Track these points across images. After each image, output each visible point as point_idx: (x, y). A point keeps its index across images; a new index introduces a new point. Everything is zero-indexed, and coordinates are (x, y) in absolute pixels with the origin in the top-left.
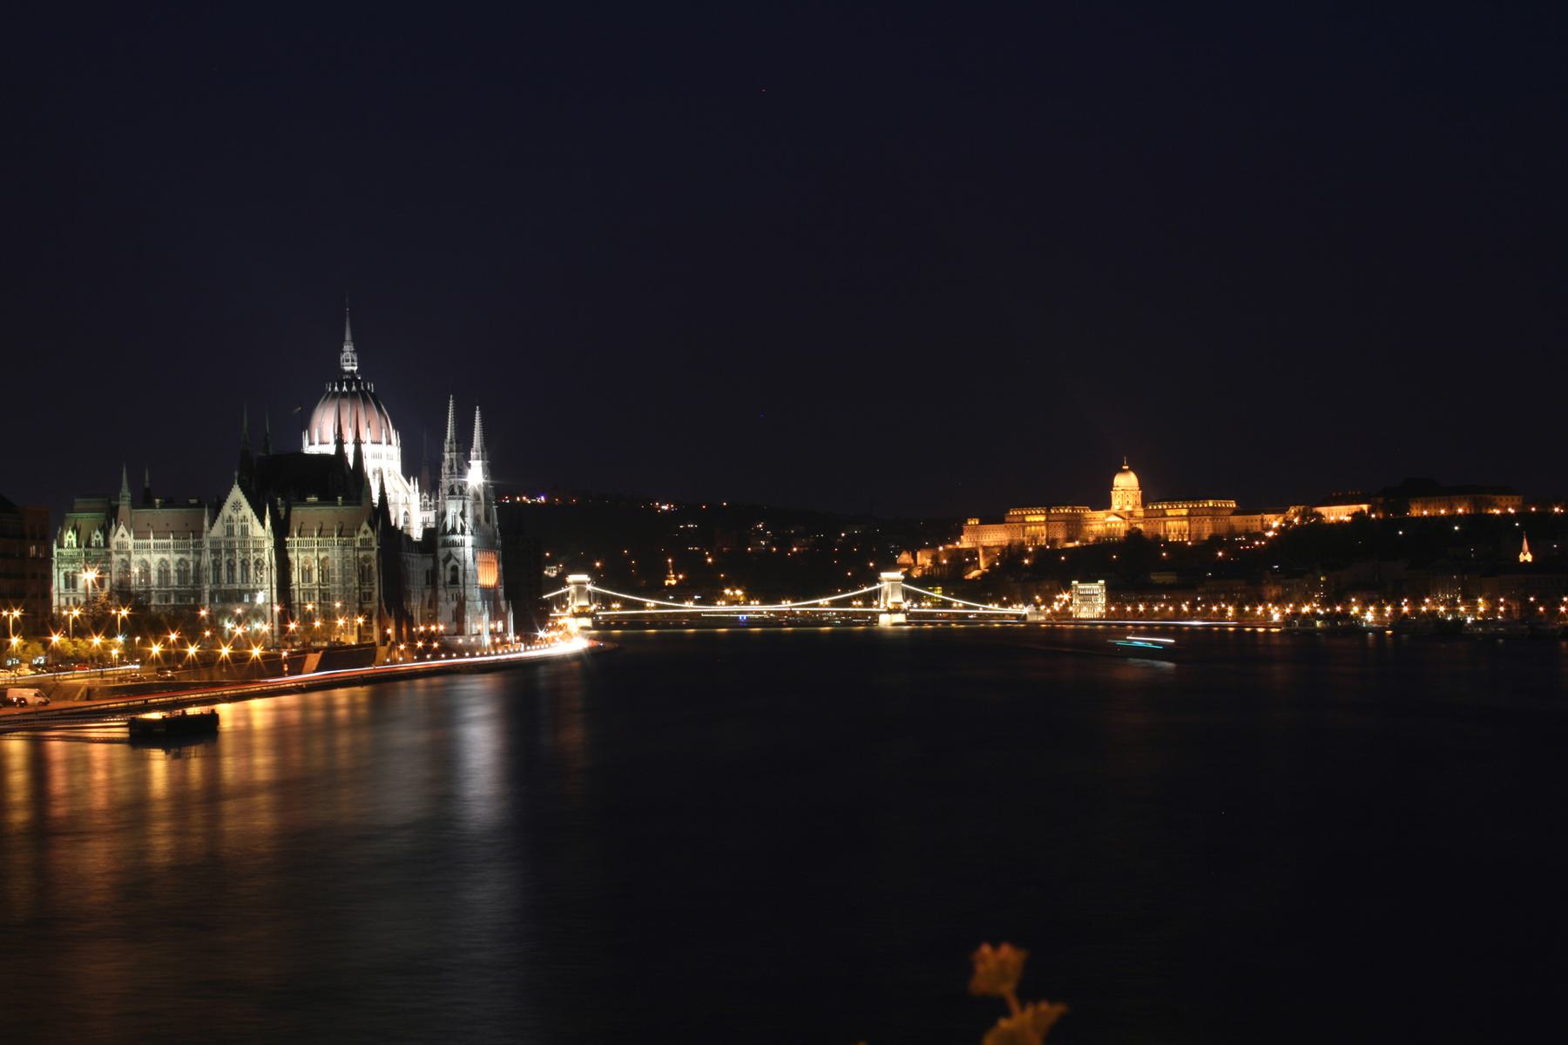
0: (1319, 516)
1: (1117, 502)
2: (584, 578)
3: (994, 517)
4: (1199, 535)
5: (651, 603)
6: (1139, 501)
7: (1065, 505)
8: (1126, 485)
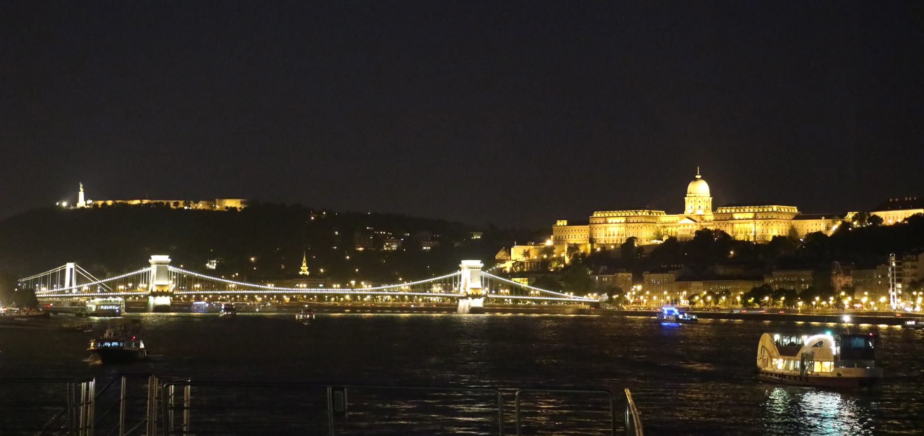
0: (880, 220)
1: (690, 205)
2: (165, 258)
3: (581, 219)
4: (763, 236)
5: (233, 284)
6: (710, 206)
7: (644, 209)
8: (699, 193)
